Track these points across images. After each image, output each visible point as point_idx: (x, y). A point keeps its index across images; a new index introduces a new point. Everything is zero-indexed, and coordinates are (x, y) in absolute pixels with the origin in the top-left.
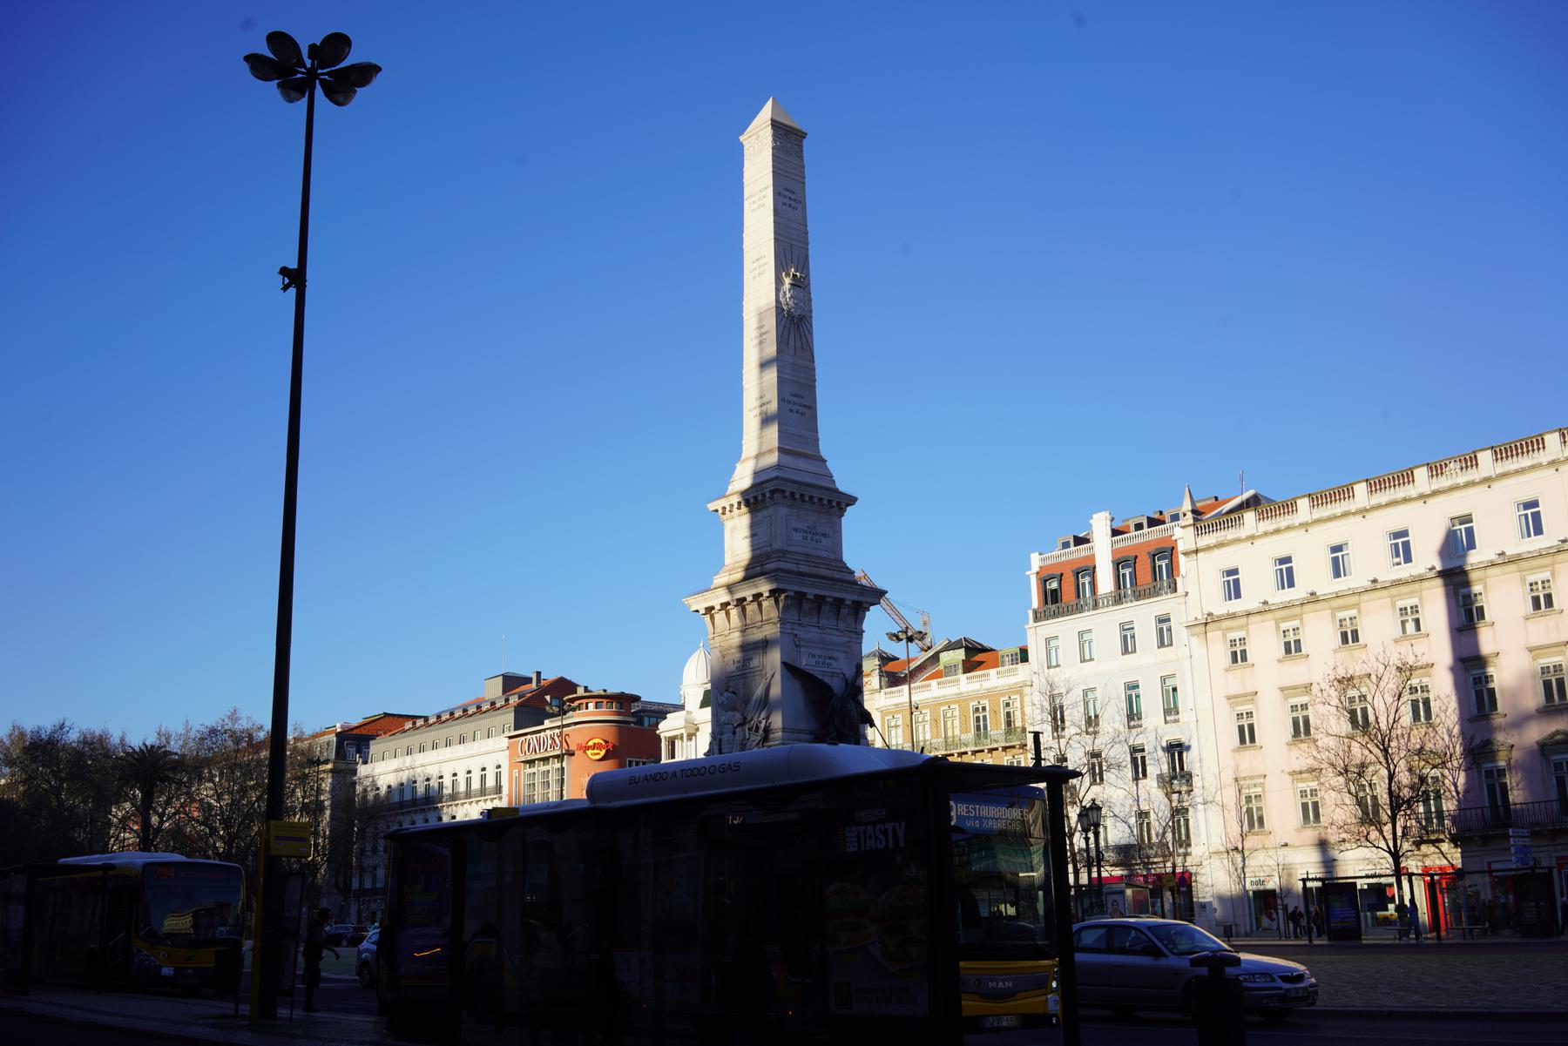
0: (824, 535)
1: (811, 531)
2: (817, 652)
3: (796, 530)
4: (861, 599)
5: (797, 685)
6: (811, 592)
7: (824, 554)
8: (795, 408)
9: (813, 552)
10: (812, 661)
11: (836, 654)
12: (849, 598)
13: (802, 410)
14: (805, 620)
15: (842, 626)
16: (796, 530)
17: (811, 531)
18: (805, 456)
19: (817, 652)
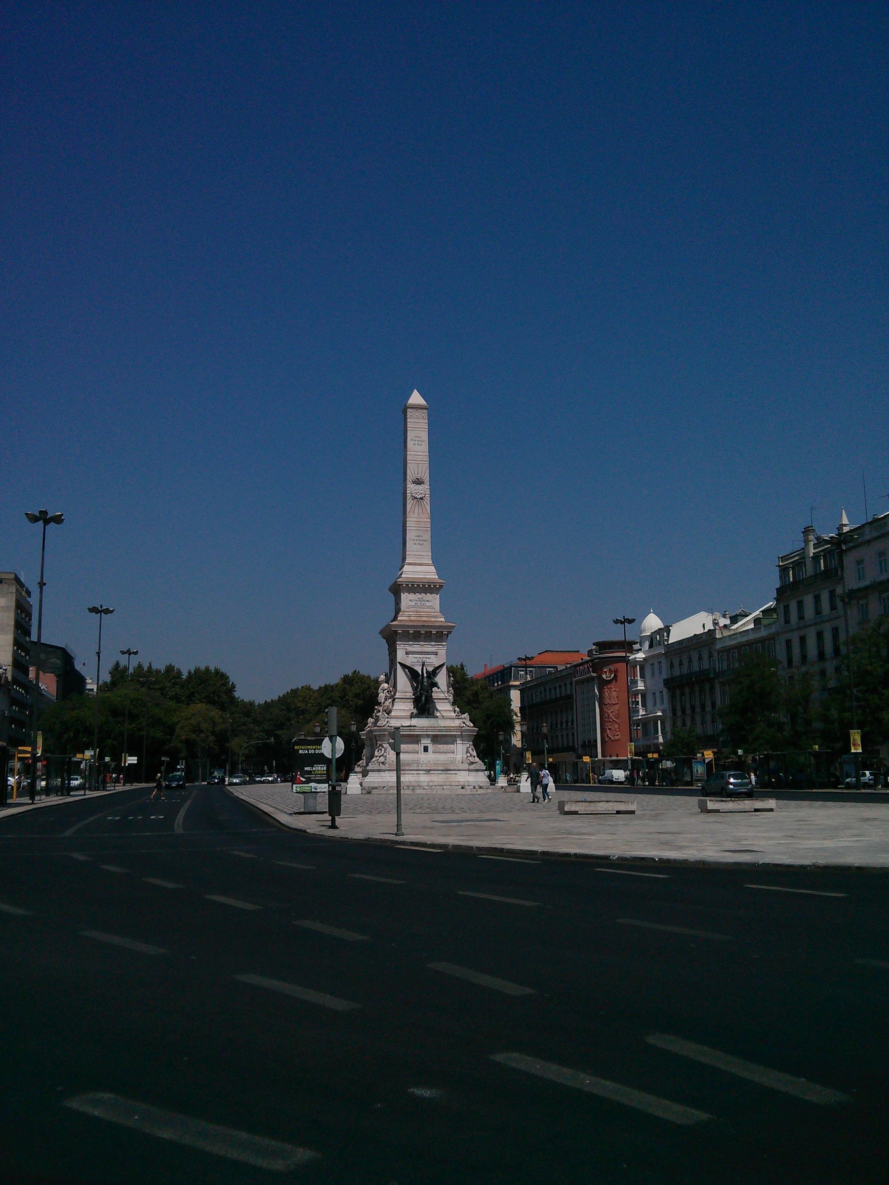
7: (428, 610)
17: (420, 600)
18: (421, 564)
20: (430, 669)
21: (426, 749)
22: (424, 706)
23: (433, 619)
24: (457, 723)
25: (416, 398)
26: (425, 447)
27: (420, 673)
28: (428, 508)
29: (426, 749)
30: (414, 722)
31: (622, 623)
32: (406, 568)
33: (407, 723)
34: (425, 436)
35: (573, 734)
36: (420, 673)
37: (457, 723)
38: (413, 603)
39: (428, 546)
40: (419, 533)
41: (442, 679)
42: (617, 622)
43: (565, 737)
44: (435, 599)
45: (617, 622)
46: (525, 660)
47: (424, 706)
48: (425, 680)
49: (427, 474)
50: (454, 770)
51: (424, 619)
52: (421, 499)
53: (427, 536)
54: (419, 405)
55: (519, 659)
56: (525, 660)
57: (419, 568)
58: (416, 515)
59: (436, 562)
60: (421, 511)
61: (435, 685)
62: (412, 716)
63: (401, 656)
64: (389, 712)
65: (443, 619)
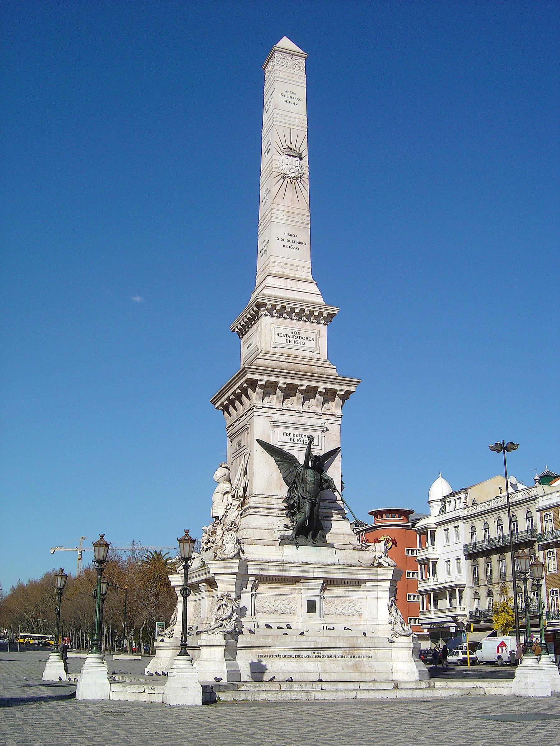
0: (309, 339)
7: (308, 354)
8: (289, 244)
9: (296, 353)
10: (287, 439)
13: (297, 245)
17: (296, 335)
21: (311, 607)
24: (367, 556)
26: (302, 107)
28: (306, 194)
30: (291, 553)
33: (274, 553)
34: (301, 92)
37: (367, 556)
38: (282, 340)
39: (305, 252)
40: (289, 230)
50: (368, 649)
51: (303, 367)
52: (297, 178)
57: (290, 284)
58: (287, 201)
59: (319, 275)
62: (284, 541)
65: (334, 372)
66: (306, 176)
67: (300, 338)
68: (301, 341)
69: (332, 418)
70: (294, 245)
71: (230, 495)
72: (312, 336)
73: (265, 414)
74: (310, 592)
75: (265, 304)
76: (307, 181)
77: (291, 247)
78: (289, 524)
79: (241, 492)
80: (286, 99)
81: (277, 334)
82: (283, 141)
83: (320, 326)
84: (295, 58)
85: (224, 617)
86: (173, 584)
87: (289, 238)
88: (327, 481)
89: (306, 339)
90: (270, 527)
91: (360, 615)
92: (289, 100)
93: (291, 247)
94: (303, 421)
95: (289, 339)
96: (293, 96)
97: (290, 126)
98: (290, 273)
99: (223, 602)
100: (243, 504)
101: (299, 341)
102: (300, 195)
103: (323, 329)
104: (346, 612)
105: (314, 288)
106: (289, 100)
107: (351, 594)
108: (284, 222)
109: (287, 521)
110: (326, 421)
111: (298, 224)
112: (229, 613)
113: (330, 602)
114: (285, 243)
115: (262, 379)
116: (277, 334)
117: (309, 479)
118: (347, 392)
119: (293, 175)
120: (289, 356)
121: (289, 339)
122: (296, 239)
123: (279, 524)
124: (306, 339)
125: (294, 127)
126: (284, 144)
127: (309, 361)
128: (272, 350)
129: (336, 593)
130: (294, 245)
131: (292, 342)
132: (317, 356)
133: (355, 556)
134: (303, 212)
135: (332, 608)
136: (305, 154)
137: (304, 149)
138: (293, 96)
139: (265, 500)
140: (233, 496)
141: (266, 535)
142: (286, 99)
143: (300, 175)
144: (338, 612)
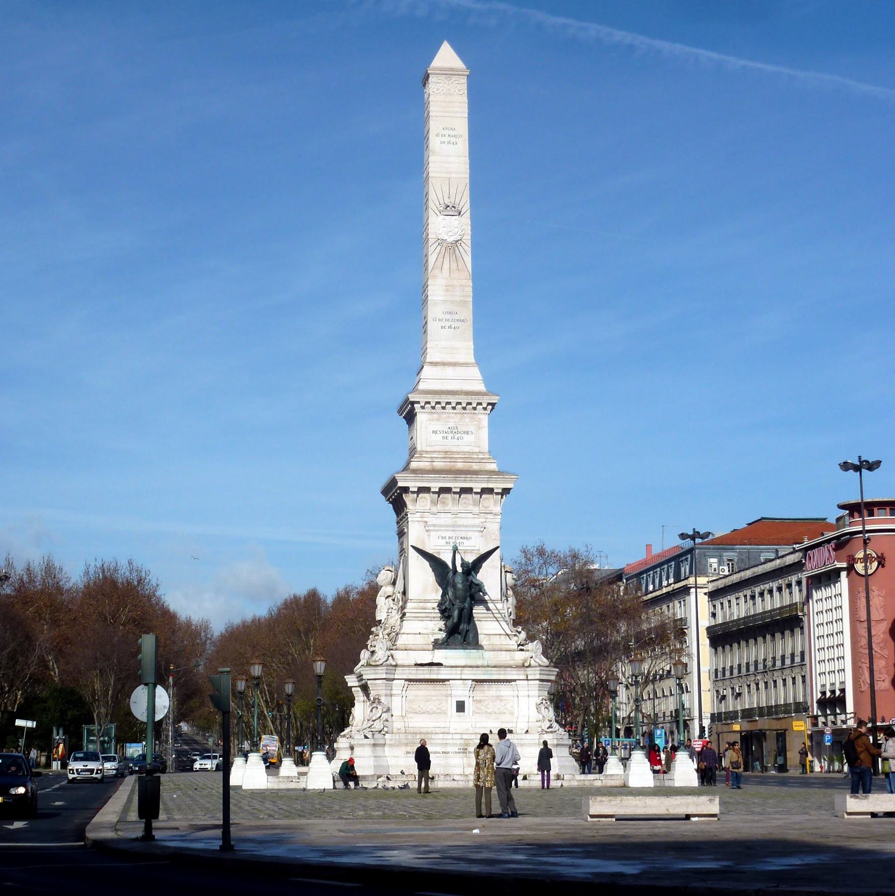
1: (454, 431)
2: (451, 534)
3: (435, 432)
4: (490, 486)
5: (427, 563)
6: (435, 486)
7: (467, 449)
8: (448, 324)
9: (454, 449)
10: (443, 542)
11: (469, 534)
12: (477, 487)
14: (434, 509)
15: (476, 510)
16: (435, 432)
17: (454, 431)
18: (455, 364)
19: (451, 534)
20: (470, 559)
21: (461, 707)
22: (459, 630)
23: (475, 467)
24: (519, 657)
25: (446, 57)
26: (462, 147)
27: (451, 566)
28: (468, 259)
29: (461, 707)
30: (440, 655)
31: (857, 468)
32: (427, 371)
33: (427, 657)
34: (462, 126)
35: (804, 677)
36: (451, 566)
37: (519, 657)
38: (439, 437)
39: (468, 329)
41: (490, 578)
42: (846, 466)
43: (789, 681)
44: (480, 428)
45: (846, 466)
46: (693, 538)
47: (459, 630)
48: (459, 580)
49: (466, 198)
53: (467, 313)
54: (452, 69)
55: (683, 536)
56: (693, 538)
57: (449, 372)
59: (481, 358)
60: (454, 266)
61: (479, 587)
62: (438, 645)
63: (415, 534)
64: (393, 637)
65: (493, 467)
66: (467, 238)
67: (458, 432)
68: (459, 435)
69: (490, 516)
70: (454, 324)
71: (390, 599)
72: (471, 428)
73: (419, 519)
74: (459, 693)
75: (418, 402)
76: (469, 243)
77: (450, 327)
78: (443, 627)
79: (399, 596)
80: (444, 139)
81: (433, 432)
82: (440, 196)
83: (481, 416)
84: (454, 78)
85: (374, 718)
86: (349, 685)
87: (448, 316)
88: (477, 585)
89: (465, 432)
90: (425, 631)
91: (512, 714)
92: (446, 139)
93: (450, 327)
94: (460, 522)
95: (445, 435)
96: (452, 133)
97: (448, 176)
98: (448, 359)
99: (375, 705)
100: (403, 608)
101: (457, 436)
102: (461, 263)
103: (484, 418)
104: (497, 711)
105: (475, 372)
106: (446, 139)
107: (503, 693)
108: (441, 298)
109: (441, 624)
110: (483, 520)
111: (458, 299)
112: (379, 715)
113: (480, 701)
114: (443, 324)
115: (413, 485)
116: (433, 432)
117: (460, 586)
118: (504, 489)
119: (450, 240)
120: (446, 452)
121: (445, 435)
122: (457, 317)
123: (435, 627)
124: (465, 432)
125: (453, 175)
126: (442, 202)
127: (468, 457)
128: (429, 449)
129: (487, 693)
130: (454, 324)
131: (449, 438)
132: (477, 450)
133: (504, 658)
134: (464, 282)
135: (483, 708)
136: (466, 207)
137: (465, 203)
138: (452, 133)
139: (421, 605)
140: (394, 600)
141: (419, 641)
142: (444, 139)
143: (459, 238)
144: (489, 711)
